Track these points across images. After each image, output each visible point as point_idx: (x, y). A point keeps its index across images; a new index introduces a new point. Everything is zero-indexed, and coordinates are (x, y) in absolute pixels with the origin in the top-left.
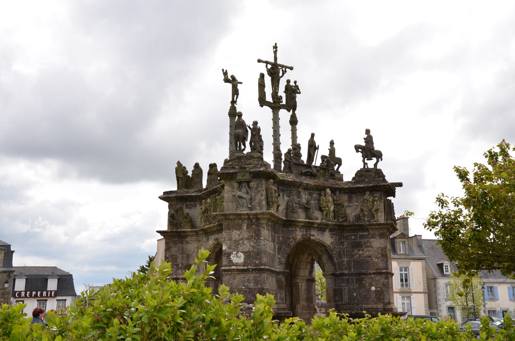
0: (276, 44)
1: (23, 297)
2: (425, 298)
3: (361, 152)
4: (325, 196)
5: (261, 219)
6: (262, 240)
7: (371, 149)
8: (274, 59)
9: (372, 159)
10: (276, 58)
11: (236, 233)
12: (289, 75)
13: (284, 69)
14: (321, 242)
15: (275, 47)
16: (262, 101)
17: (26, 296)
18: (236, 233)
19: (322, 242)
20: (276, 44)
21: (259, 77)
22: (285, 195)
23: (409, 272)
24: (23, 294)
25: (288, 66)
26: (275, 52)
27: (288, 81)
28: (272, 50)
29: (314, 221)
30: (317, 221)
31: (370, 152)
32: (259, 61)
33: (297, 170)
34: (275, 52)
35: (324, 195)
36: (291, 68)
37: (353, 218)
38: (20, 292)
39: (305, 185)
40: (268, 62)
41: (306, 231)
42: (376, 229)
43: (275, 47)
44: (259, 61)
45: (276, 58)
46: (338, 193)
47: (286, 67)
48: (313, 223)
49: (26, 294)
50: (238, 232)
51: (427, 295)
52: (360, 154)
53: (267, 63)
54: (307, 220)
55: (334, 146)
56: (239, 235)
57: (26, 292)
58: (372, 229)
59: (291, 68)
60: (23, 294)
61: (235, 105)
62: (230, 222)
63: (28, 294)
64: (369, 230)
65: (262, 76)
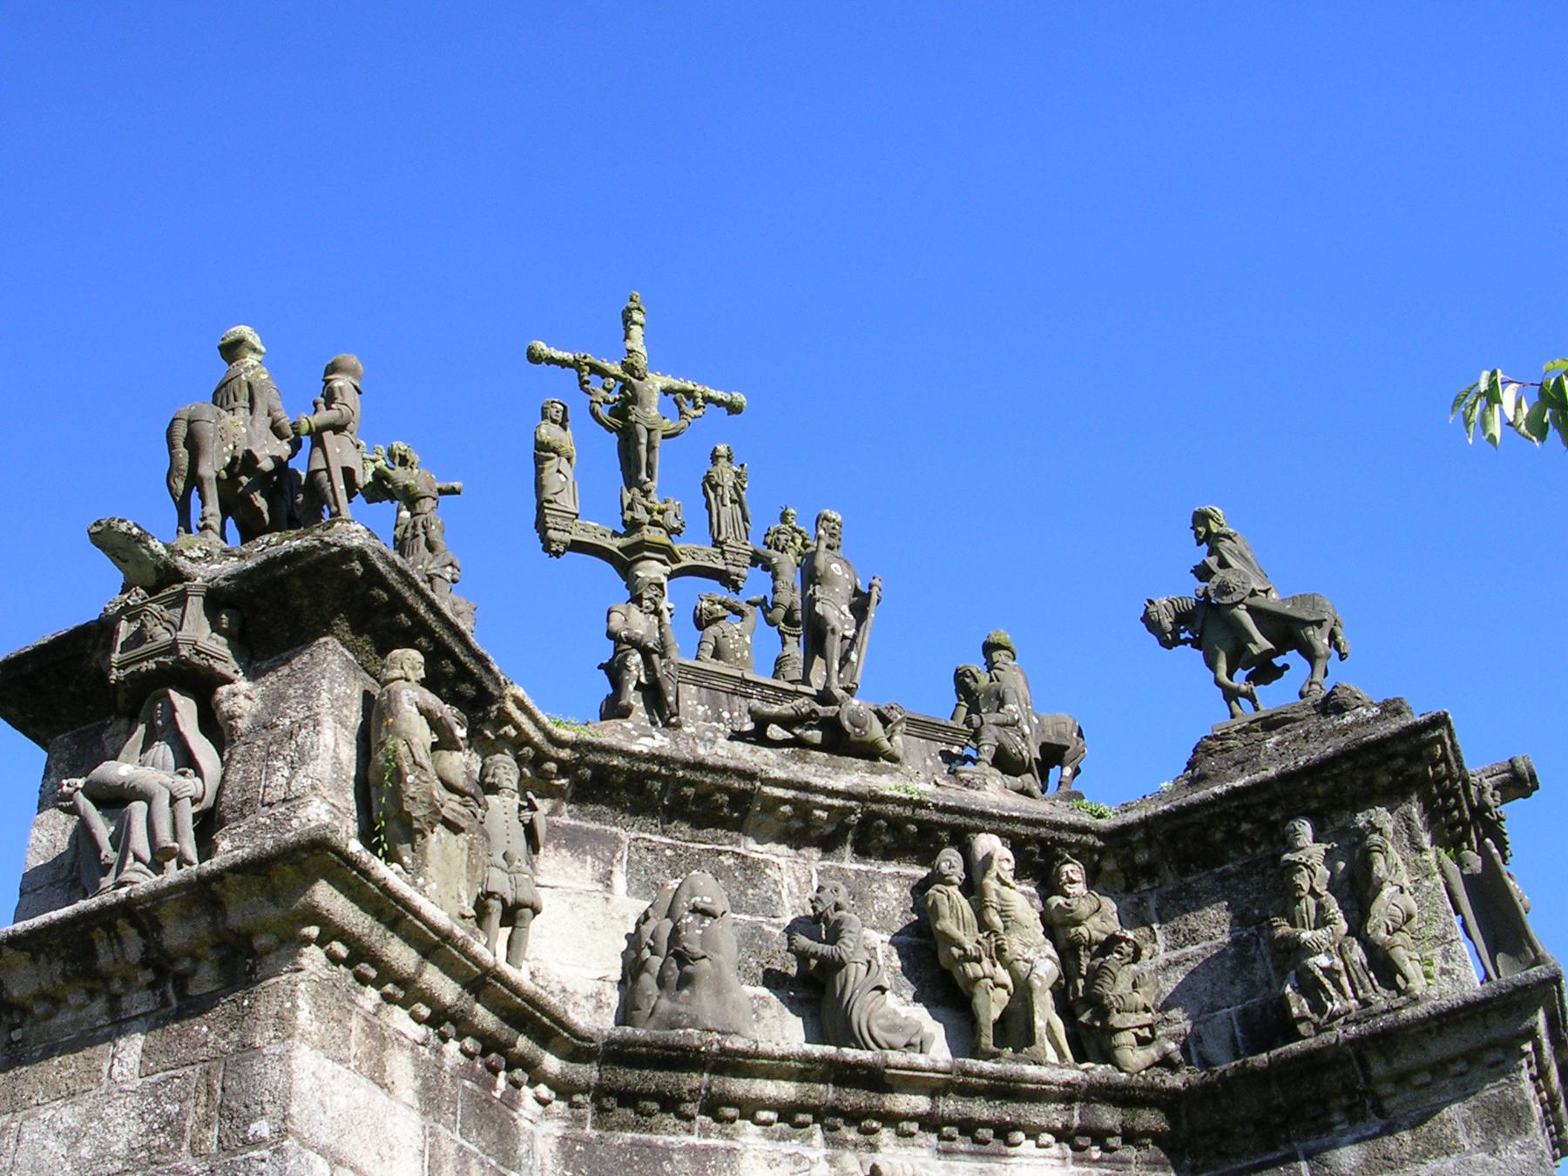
3: (1197, 644)
4: (972, 888)
5: (261, 942)
6: (258, 1143)
9: (1278, 672)
11: (51, 1124)
18: (51, 1124)
22: (620, 880)
29: (895, 1057)
30: (920, 1060)
33: (720, 719)
35: (957, 873)
37: (1233, 1038)
39: (779, 792)
41: (831, 1161)
46: (1073, 870)
48: (876, 1079)
50: (68, 1116)
52: (1190, 657)
54: (818, 1050)
56: (74, 1138)
58: (1402, 1078)
62: (16, 1035)
64: (1387, 1089)
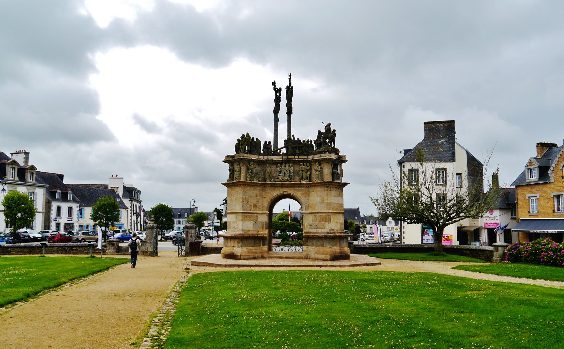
0: (291, 74)
2: (43, 217)
15: (290, 76)
20: (291, 74)
23: (34, 197)
26: (290, 79)
28: (288, 77)
34: (290, 79)
43: (290, 76)
51: (44, 214)
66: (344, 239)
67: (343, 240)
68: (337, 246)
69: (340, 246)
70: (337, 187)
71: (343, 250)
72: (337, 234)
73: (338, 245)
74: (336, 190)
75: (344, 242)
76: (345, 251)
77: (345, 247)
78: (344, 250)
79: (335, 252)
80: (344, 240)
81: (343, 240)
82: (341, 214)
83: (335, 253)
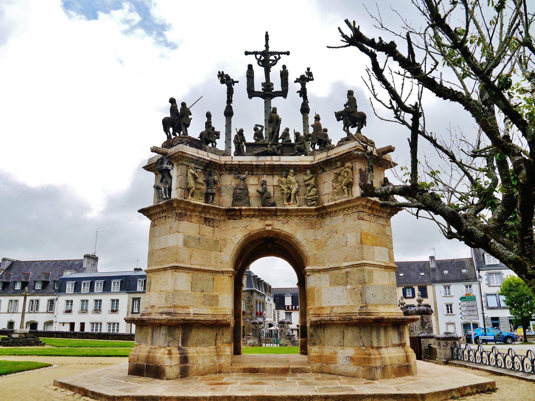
1: (290, 310)
7: (350, 112)
8: (275, 51)
10: (267, 46)
12: (284, 60)
13: (277, 56)
14: (283, 232)
15: (267, 37)
16: (252, 93)
17: (292, 309)
19: (284, 233)
21: (247, 69)
24: (290, 308)
25: (283, 51)
27: (284, 67)
31: (349, 116)
32: (247, 53)
36: (288, 53)
38: (288, 306)
40: (257, 52)
42: (349, 208)
43: (267, 37)
44: (247, 53)
45: (267, 46)
47: (279, 53)
49: (292, 308)
53: (256, 53)
55: (320, 121)
57: (292, 306)
59: (288, 53)
60: (290, 308)
61: (231, 104)
63: (294, 308)
65: (250, 67)
66: (160, 329)
67: (159, 330)
68: (146, 342)
69: (152, 344)
70: (164, 215)
71: (154, 353)
72: (155, 315)
73: (149, 342)
74: (164, 221)
75: (160, 335)
76: (155, 357)
77: (161, 347)
78: (155, 355)
79: (138, 355)
80: (160, 331)
81: (159, 330)
82: (170, 271)
83: (138, 359)
